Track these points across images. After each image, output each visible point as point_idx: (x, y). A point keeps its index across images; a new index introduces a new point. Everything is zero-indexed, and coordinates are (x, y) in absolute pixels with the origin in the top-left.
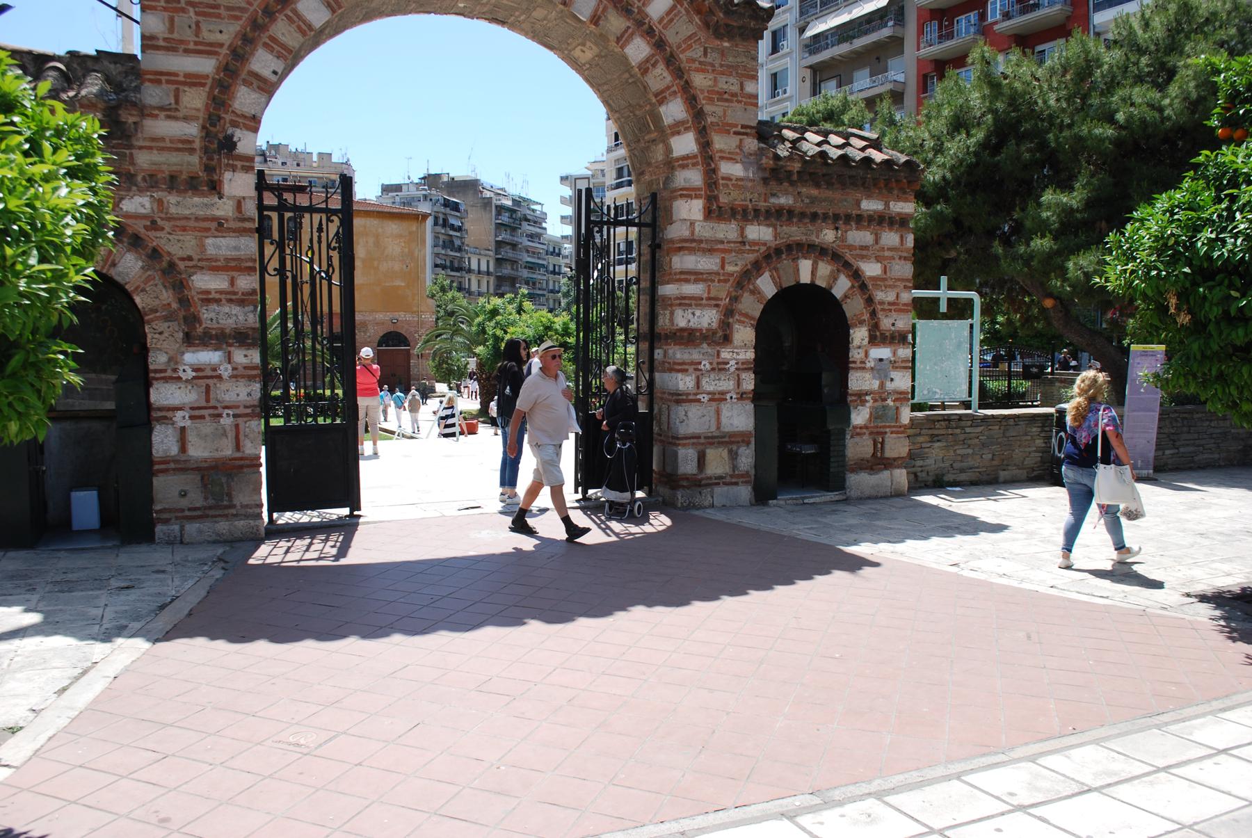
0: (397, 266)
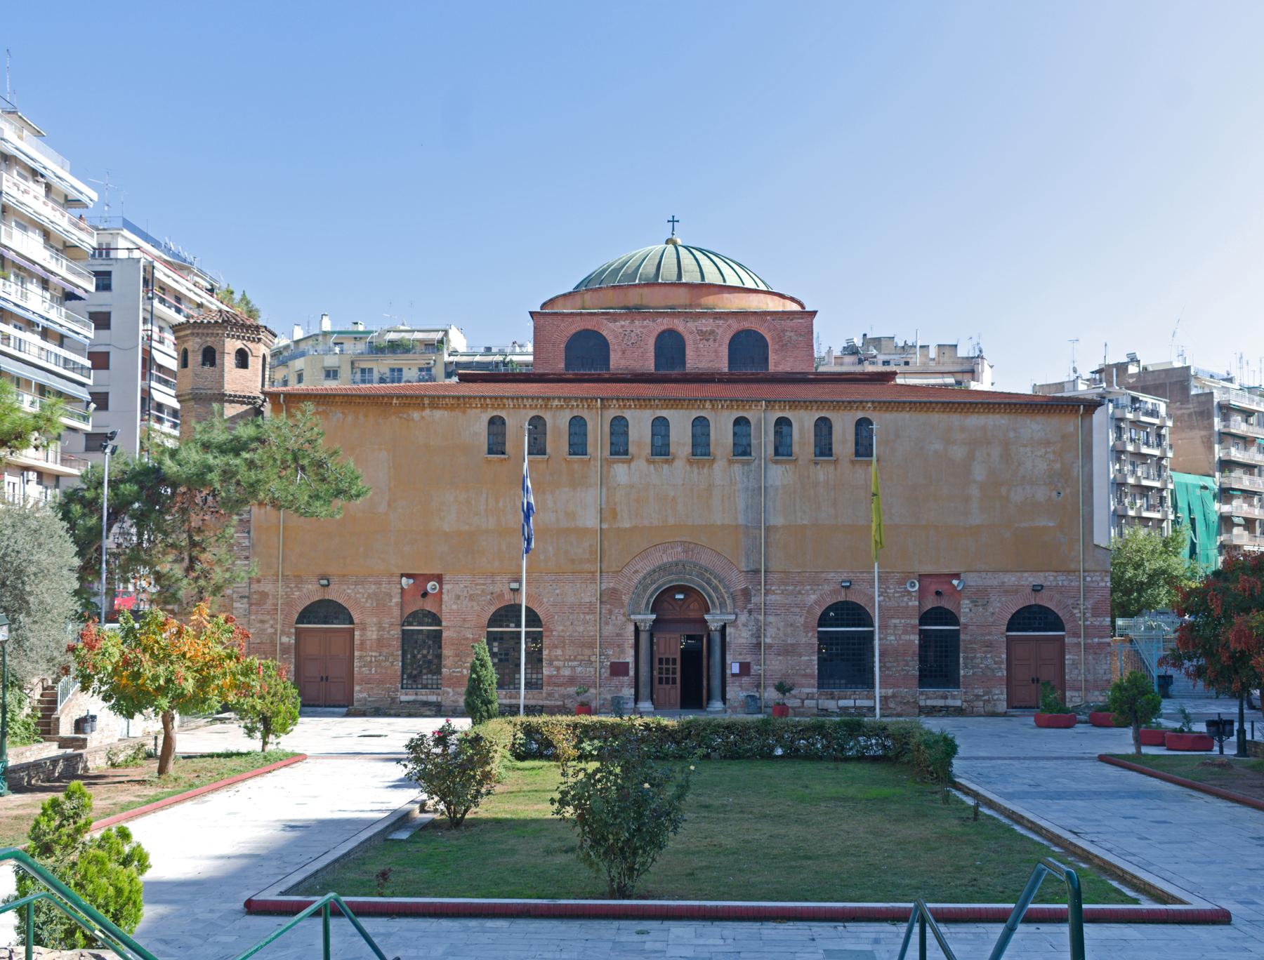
0: (1041, 494)
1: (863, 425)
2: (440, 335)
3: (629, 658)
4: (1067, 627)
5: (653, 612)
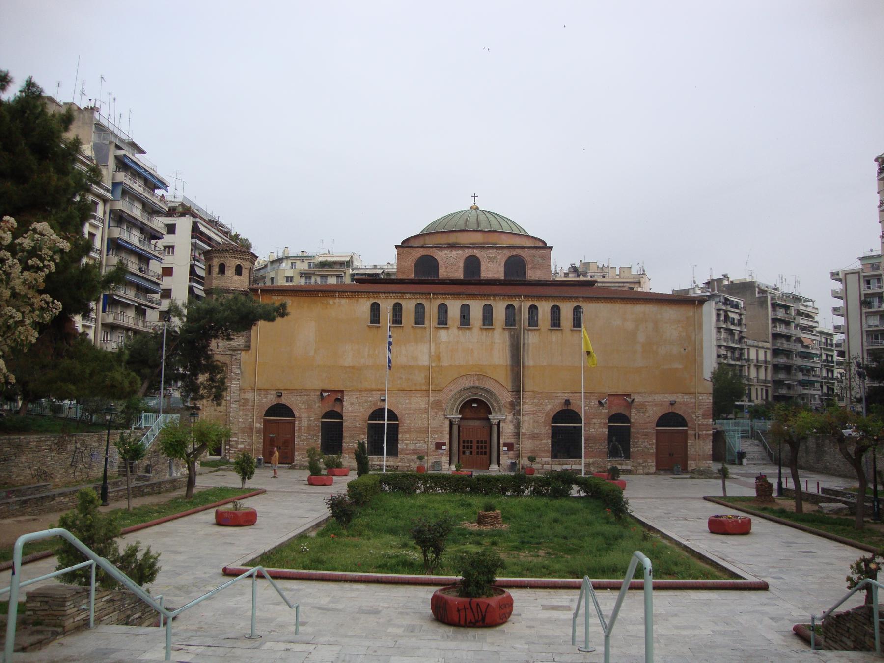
1: (577, 310)
2: (347, 259)
3: (446, 439)
4: (689, 425)
5: (460, 413)
